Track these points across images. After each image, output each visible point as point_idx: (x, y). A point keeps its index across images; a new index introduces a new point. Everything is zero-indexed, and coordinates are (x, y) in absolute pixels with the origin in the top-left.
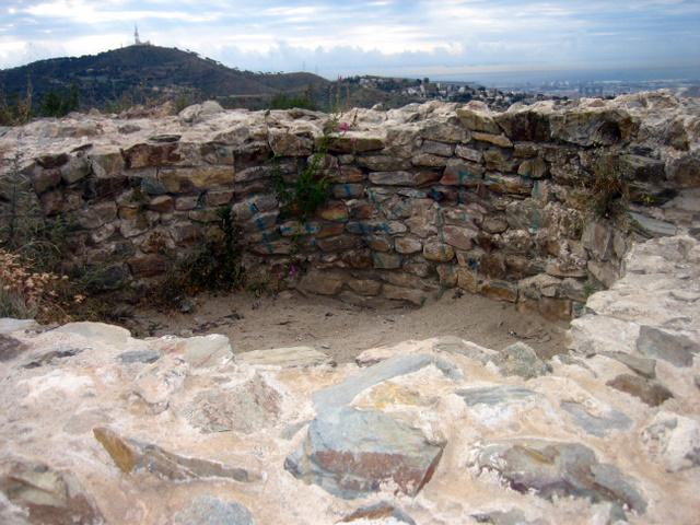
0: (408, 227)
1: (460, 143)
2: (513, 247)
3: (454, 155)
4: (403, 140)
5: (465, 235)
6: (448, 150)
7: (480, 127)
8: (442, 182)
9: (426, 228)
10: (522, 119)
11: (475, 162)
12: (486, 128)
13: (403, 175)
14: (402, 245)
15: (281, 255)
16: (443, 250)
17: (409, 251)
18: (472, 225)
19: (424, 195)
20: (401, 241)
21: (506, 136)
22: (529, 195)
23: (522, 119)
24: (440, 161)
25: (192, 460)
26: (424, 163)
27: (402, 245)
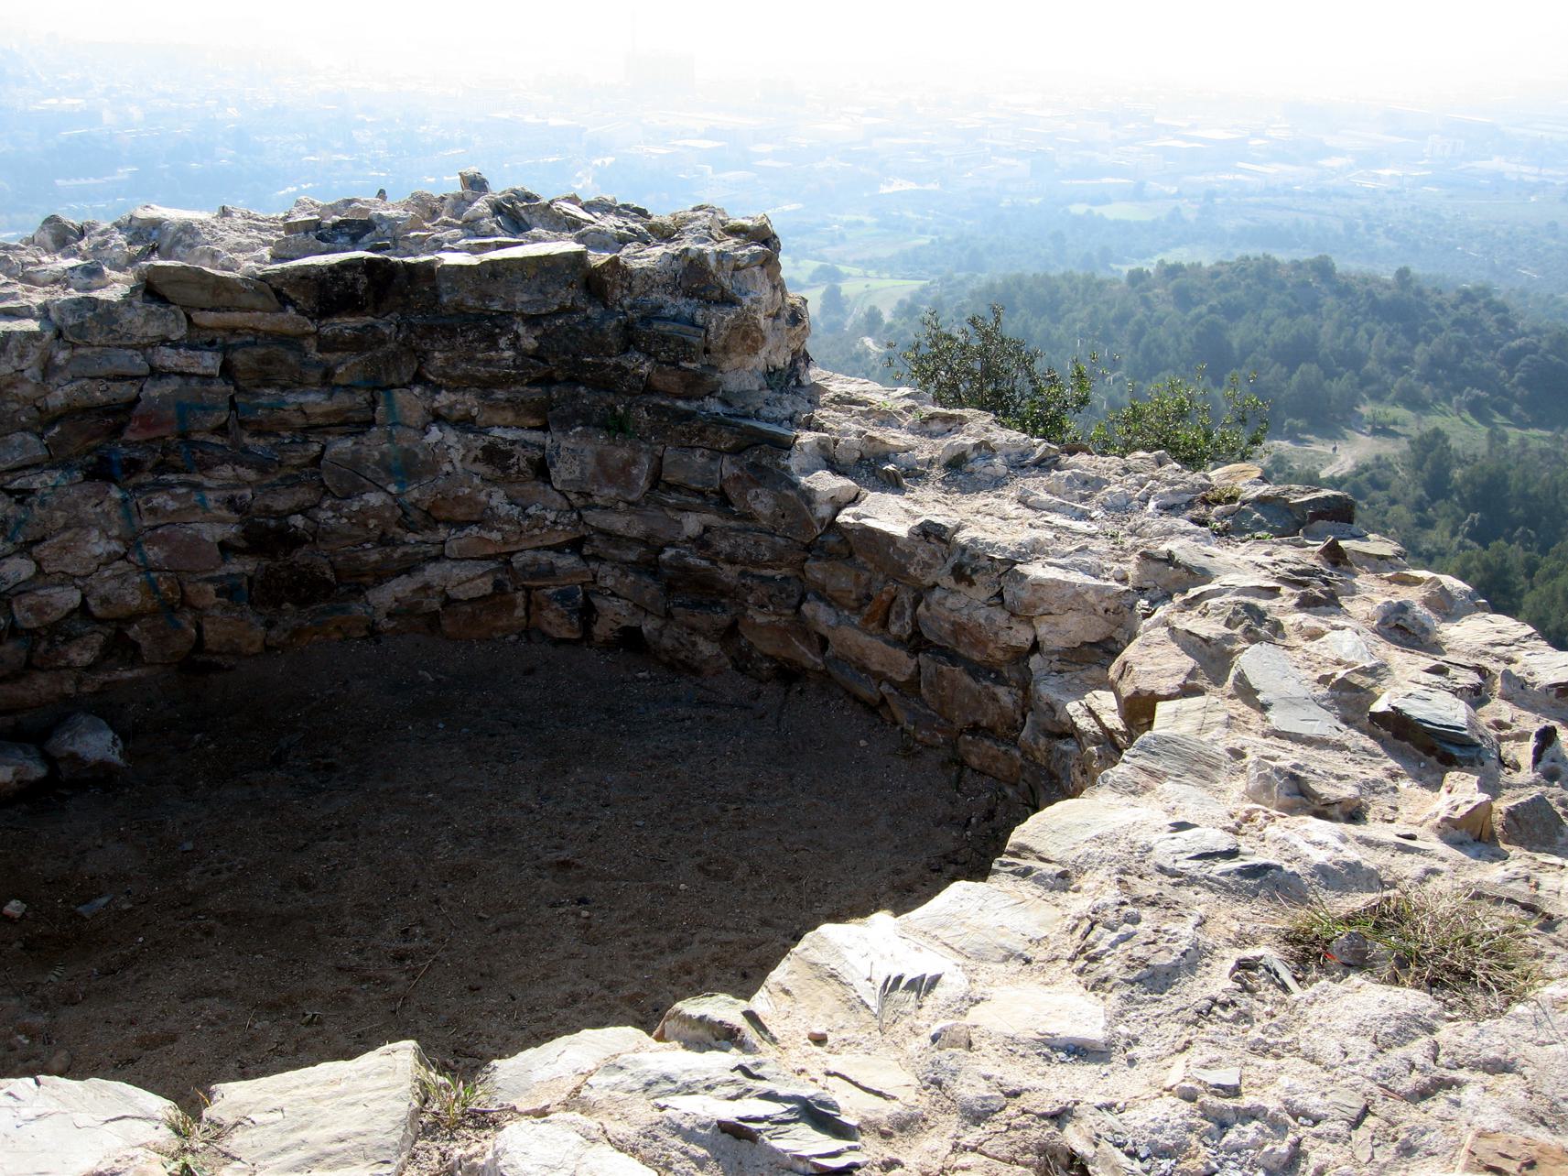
0: (38, 563)
1: (164, 341)
2: (356, 531)
3: (157, 373)
4: (22, 357)
5: (207, 537)
6: (139, 363)
7: (225, 298)
8: (129, 436)
9: (98, 550)
10: (348, 275)
11: (210, 377)
12: (246, 300)
13: (23, 445)
14: (30, 609)
15: (681, 605)
16: (152, 587)
17: (54, 616)
18: (224, 513)
19: (78, 475)
20: (28, 600)
21: (300, 312)
22: (372, 423)
23: (348, 275)
24: (124, 391)
25: (701, 1019)
26: (84, 400)
27: (30, 609)
